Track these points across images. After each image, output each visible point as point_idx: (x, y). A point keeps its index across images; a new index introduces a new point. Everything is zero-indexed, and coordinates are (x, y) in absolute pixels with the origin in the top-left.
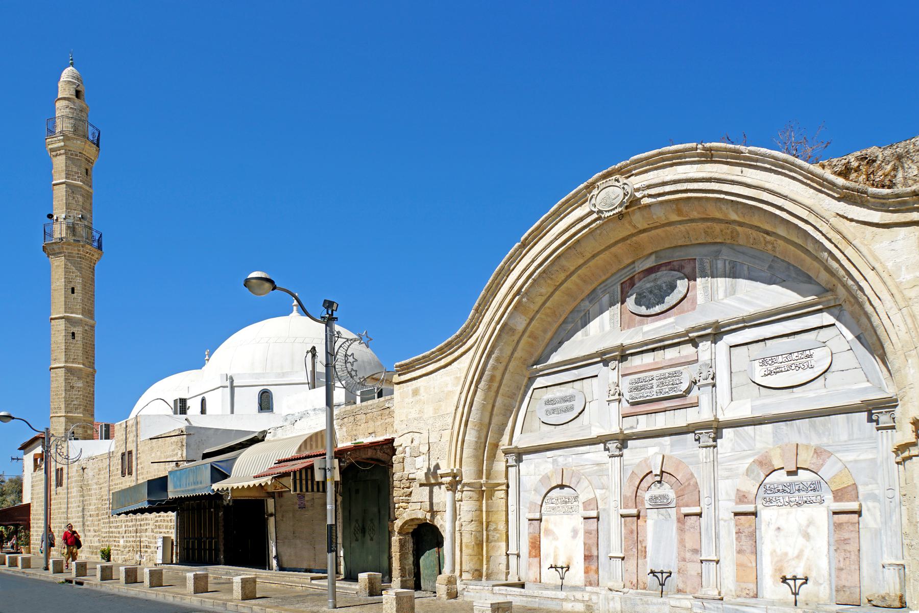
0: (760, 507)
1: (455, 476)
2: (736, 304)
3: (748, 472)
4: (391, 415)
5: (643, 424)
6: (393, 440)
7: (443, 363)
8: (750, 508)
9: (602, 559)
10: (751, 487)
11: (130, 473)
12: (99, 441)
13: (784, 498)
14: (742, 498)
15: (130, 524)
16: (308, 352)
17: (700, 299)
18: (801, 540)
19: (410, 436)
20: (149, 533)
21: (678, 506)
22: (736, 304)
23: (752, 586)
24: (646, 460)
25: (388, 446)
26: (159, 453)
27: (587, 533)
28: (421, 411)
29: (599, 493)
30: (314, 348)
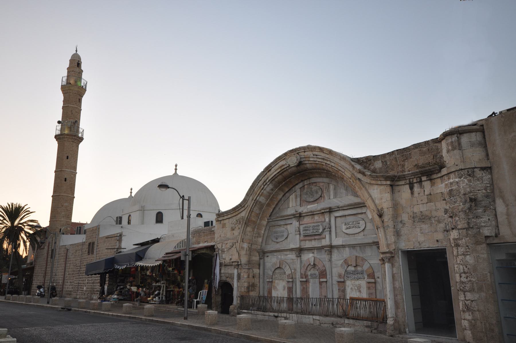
1: (238, 262)
3: (342, 265)
4: (214, 234)
5: (308, 244)
7: (234, 214)
8: (342, 280)
11: (93, 253)
14: (340, 276)
15: (91, 279)
24: (309, 259)
25: (212, 248)
26: (108, 244)
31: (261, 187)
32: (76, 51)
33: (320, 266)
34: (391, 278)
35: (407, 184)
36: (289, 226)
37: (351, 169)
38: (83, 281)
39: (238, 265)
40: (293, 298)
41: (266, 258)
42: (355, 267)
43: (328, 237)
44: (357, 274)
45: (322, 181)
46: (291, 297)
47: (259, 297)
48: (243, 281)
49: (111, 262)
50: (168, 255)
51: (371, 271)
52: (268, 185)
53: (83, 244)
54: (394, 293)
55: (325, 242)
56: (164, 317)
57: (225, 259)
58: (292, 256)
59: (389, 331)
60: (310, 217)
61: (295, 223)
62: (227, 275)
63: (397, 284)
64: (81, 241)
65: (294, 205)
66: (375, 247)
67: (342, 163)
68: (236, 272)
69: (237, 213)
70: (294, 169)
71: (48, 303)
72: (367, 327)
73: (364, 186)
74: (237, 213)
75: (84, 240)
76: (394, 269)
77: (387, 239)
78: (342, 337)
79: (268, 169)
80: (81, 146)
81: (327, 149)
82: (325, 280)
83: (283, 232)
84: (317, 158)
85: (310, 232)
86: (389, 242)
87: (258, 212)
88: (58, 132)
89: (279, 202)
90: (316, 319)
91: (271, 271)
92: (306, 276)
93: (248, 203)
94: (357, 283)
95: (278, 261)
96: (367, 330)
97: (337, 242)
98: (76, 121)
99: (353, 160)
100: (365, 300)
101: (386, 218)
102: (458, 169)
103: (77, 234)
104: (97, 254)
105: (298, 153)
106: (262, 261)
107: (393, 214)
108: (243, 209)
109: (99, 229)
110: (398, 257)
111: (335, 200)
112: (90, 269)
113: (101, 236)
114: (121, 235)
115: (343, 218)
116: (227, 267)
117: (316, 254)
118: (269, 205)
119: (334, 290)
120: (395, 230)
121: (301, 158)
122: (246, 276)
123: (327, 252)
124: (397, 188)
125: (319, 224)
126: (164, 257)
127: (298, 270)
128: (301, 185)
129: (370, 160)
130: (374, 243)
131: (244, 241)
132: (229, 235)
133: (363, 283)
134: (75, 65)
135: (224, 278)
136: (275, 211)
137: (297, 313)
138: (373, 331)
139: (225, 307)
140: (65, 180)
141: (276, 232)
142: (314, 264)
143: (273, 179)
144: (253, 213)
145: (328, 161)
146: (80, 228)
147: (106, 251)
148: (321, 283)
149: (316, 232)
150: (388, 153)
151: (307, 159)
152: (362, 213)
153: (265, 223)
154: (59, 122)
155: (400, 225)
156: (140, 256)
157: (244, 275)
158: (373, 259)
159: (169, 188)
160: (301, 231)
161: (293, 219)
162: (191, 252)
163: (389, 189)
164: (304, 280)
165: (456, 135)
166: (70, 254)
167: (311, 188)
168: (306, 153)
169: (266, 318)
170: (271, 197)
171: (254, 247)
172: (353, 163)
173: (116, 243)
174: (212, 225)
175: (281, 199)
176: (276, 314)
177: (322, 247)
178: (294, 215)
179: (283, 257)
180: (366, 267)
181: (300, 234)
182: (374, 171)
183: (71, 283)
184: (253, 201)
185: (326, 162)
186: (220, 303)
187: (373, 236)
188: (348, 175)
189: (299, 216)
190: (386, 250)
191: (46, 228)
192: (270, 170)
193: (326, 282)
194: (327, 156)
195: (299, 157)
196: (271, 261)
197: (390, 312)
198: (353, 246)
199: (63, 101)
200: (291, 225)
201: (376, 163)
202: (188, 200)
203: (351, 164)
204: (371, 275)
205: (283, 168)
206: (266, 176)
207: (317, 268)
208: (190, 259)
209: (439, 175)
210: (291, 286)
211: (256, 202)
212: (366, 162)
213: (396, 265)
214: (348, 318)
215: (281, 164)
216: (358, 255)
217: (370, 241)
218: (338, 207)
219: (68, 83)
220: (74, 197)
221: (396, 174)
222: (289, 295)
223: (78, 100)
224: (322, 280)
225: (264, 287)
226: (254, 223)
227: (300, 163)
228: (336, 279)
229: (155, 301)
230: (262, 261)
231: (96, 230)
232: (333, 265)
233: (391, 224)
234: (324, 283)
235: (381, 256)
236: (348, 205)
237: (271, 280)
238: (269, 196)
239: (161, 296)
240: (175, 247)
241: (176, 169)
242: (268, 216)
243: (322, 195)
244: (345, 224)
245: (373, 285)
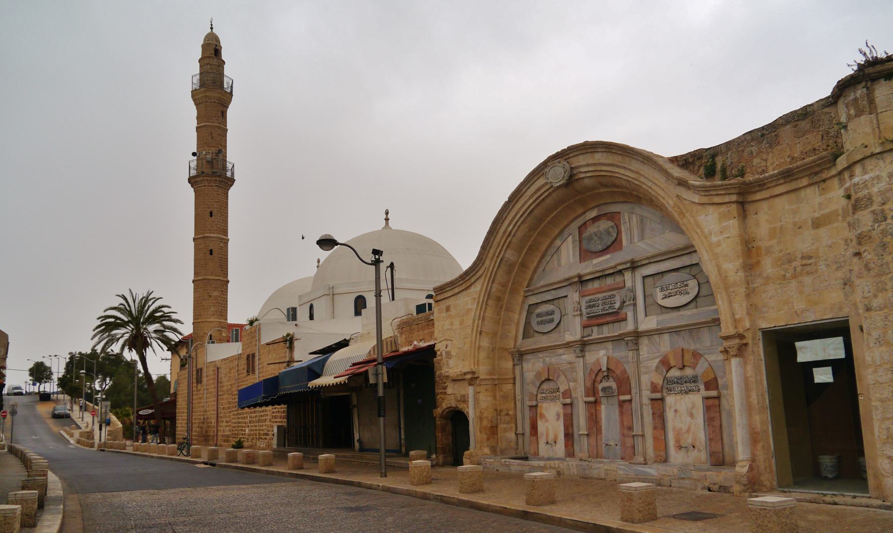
0: (665, 394)
1: (474, 373)
2: (645, 247)
3: (657, 368)
6: (434, 345)
7: (464, 287)
8: (658, 395)
9: (576, 436)
10: (659, 381)
11: (254, 372)
13: (678, 388)
14: (654, 388)
17: (624, 243)
18: (689, 419)
19: (445, 343)
20: (268, 423)
21: (619, 395)
22: (645, 247)
23: (663, 454)
24: (598, 360)
25: (430, 351)
27: (565, 415)
28: (452, 324)
29: (571, 384)
30: (392, 264)
32: (212, 28)
38: (244, 418)
41: (525, 365)
44: (686, 385)
53: (239, 357)
64: (236, 353)
75: (240, 352)
76: (749, 368)
78: (631, 500)
80: (232, 192)
85: (598, 310)
86: (737, 317)
88: (194, 173)
97: (648, 323)
98: (220, 151)
102: (868, 154)
109: (259, 330)
111: (640, 244)
119: (645, 415)
121: (572, 169)
123: (630, 344)
124: (751, 208)
134: (212, 52)
140: (211, 252)
142: (608, 369)
146: (237, 330)
148: (622, 404)
154: (194, 154)
156: (314, 371)
159: (337, 244)
160: (583, 309)
164: (592, 399)
165: (863, 84)
180: (701, 368)
181: (581, 315)
190: (732, 331)
191: (190, 335)
193: (630, 401)
196: (532, 367)
198: (675, 331)
199: (197, 118)
200: (566, 299)
204: (712, 384)
209: (833, 172)
216: (686, 346)
219: (203, 83)
220: (228, 282)
223: (220, 114)
224: (622, 398)
227: (571, 179)
228: (647, 394)
232: (642, 370)
234: (627, 404)
240: (370, 352)
241: (387, 219)
244: (662, 290)
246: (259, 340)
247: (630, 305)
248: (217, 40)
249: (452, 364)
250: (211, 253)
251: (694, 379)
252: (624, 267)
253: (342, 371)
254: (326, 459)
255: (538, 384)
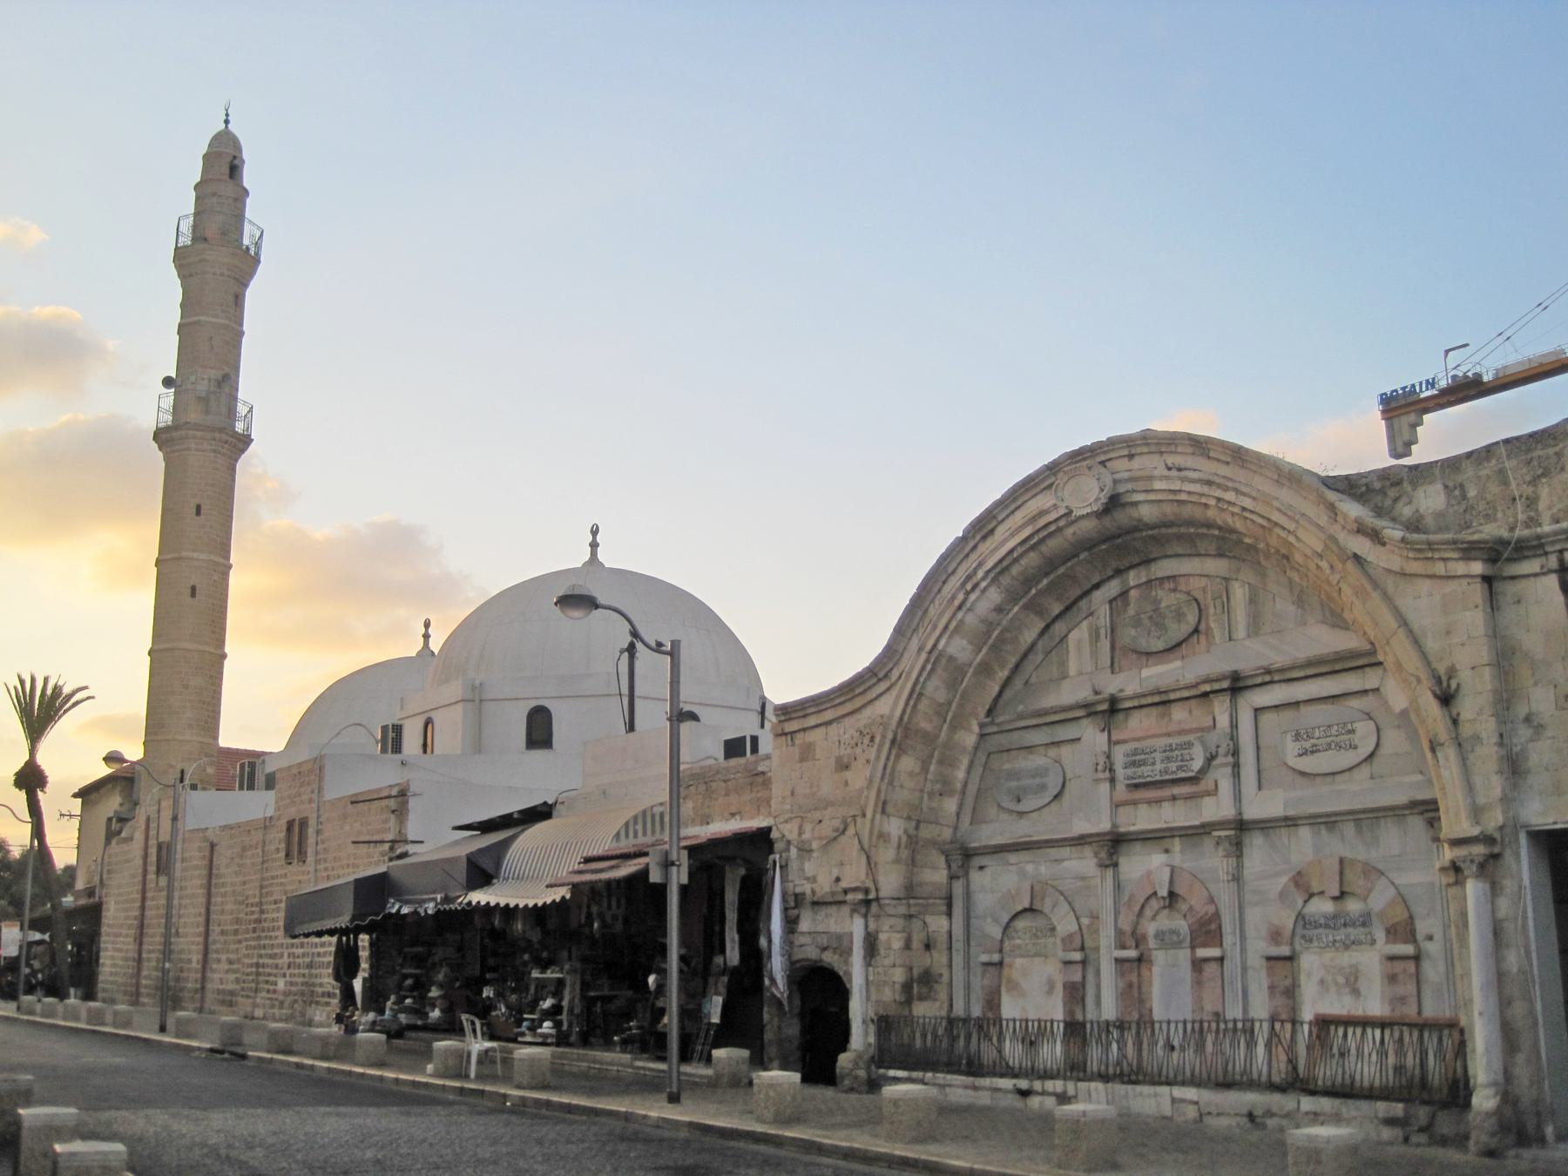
0: (1298, 947)
1: (867, 891)
3: (1283, 895)
4: (767, 783)
5: (1143, 819)
6: (769, 829)
7: (849, 707)
8: (1285, 950)
12: (237, 793)
14: (1275, 936)
15: (300, 951)
16: (622, 652)
24: (1149, 873)
25: (761, 840)
26: (357, 826)
31: (953, 598)
32: (227, 122)
33: (1195, 900)
34: (1490, 936)
35: (1551, 571)
36: (1065, 751)
37: (1323, 520)
39: (867, 904)
40: (1083, 1025)
41: (975, 876)
42: (1335, 899)
43: (1225, 786)
44: (1345, 928)
45: (1198, 570)
46: (1079, 1017)
47: (951, 1022)
48: (887, 962)
49: (374, 890)
50: (594, 866)
51: (1400, 914)
52: (984, 591)
53: (267, 824)
54: (1500, 993)
55: (1218, 808)
56: (593, 1092)
57: (813, 880)
58: (1084, 863)
59: (1480, 1137)
60: (1154, 711)
61: (1092, 736)
62: (824, 941)
63: (1512, 960)
64: (261, 816)
65: (1089, 668)
66: (1416, 823)
67: (1286, 495)
68: (857, 927)
69: (858, 703)
70: (1089, 526)
71: (163, 1029)
72: (1390, 1122)
73: (1375, 585)
74: (858, 703)
77: (1470, 788)
78: (1319, 1162)
79: (983, 527)
81: (1224, 445)
82: (1214, 952)
83: (1040, 772)
84: (1183, 480)
86: (1481, 800)
87: (941, 696)
88: (167, 419)
89: (1025, 655)
90: (1183, 1101)
91: (996, 921)
92: (1139, 941)
93: (905, 664)
94: (1346, 959)
95: (1026, 886)
96: (1387, 1133)
98: (226, 377)
99: (1331, 483)
100: (1383, 1025)
101: (1468, 707)
103: (241, 788)
104: (317, 862)
105: (1103, 463)
106: (958, 887)
107: (1495, 692)
108: (883, 686)
109: (321, 769)
110: (1517, 855)
111: (1254, 645)
112: (302, 916)
113: (330, 794)
114: (403, 794)
115: (1288, 714)
116: (824, 911)
117: (1179, 853)
118: (985, 669)
119: (1253, 988)
120: (1503, 752)
121: (1115, 482)
122: (897, 944)
123: (1226, 844)
124: (1509, 589)
125: (1190, 738)
126: (580, 872)
127: (1107, 918)
128: (1113, 588)
129: (1398, 483)
130: (1414, 805)
131: (889, 809)
132: (827, 788)
133: (1370, 960)
135: (811, 953)
136: (1008, 694)
137: (1105, 1078)
138: (1414, 1139)
139: (818, 1057)
141: (1014, 775)
142: (1172, 894)
143: (1002, 568)
144: (925, 702)
145: (1226, 489)
146: (252, 765)
147: (351, 849)
148: (1198, 965)
149: (1180, 768)
150: (1469, 455)
151: (1140, 486)
152: (1365, 692)
153: (969, 739)
154: (168, 382)
155: (1524, 733)
157: (891, 939)
158: (1410, 867)
159: (597, 607)
161: (1085, 722)
162: (685, 853)
163: (1477, 591)
164: (1132, 953)
166: (221, 861)
167: (1157, 602)
168: (1136, 464)
169: (984, 1099)
170: (993, 639)
171: (926, 832)
172: (1332, 496)
173: (386, 821)
174: (755, 750)
175: (1033, 645)
176: (1023, 1084)
177: (1205, 829)
178: (1085, 706)
179: (1043, 869)
180: (1380, 898)
181: (1112, 780)
182: (1415, 525)
183: (230, 962)
184: (924, 656)
185: (1219, 493)
186: (796, 1043)
187: (1407, 779)
188: (1311, 541)
189: (1111, 710)
190: (1468, 829)
192: (992, 531)
193: (1221, 959)
194: (1224, 470)
195: (1108, 480)
196: (994, 886)
197: (1483, 1066)
198: (1328, 822)
199: (182, 306)
200: (1076, 746)
201: (1420, 493)
202: (671, 654)
203: (1322, 500)
204: (1403, 930)
205: (1042, 522)
206: (973, 556)
207: (1184, 907)
208: (685, 880)
210: (1077, 977)
211: (936, 658)
212: (1382, 491)
213: (1509, 884)
214: (1313, 1093)
215: (1033, 506)
216: (1348, 854)
217: (1401, 798)
218: (1268, 672)
219: (199, 235)
220: (224, 656)
221: (1505, 534)
222: (1070, 1012)
223: (231, 299)
224: (1202, 953)
225: (968, 987)
226: (929, 739)
227: (1114, 502)
228: (1259, 947)
229: (545, 1036)
230: (958, 887)
231: (310, 771)
232: (1248, 897)
233: (1487, 728)
235: (1448, 854)
236: (1310, 663)
237: (996, 958)
238: (988, 634)
239: (564, 1017)
240: (618, 835)
241: (594, 545)
242: (982, 712)
243: (1202, 627)
245: (1408, 968)
246: (320, 790)
247: (1225, 765)
248: (237, 145)
249: (808, 869)
250: (193, 594)
251: (1365, 921)
252: (1217, 686)
253: (563, 873)
254: (532, 1060)
255: (1006, 919)
